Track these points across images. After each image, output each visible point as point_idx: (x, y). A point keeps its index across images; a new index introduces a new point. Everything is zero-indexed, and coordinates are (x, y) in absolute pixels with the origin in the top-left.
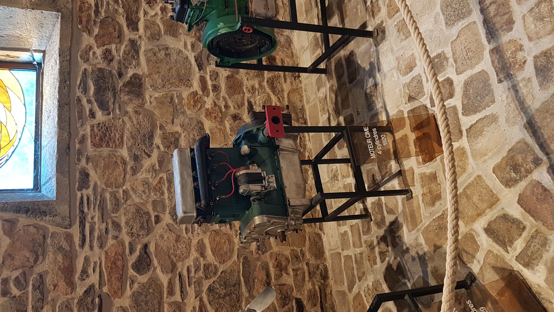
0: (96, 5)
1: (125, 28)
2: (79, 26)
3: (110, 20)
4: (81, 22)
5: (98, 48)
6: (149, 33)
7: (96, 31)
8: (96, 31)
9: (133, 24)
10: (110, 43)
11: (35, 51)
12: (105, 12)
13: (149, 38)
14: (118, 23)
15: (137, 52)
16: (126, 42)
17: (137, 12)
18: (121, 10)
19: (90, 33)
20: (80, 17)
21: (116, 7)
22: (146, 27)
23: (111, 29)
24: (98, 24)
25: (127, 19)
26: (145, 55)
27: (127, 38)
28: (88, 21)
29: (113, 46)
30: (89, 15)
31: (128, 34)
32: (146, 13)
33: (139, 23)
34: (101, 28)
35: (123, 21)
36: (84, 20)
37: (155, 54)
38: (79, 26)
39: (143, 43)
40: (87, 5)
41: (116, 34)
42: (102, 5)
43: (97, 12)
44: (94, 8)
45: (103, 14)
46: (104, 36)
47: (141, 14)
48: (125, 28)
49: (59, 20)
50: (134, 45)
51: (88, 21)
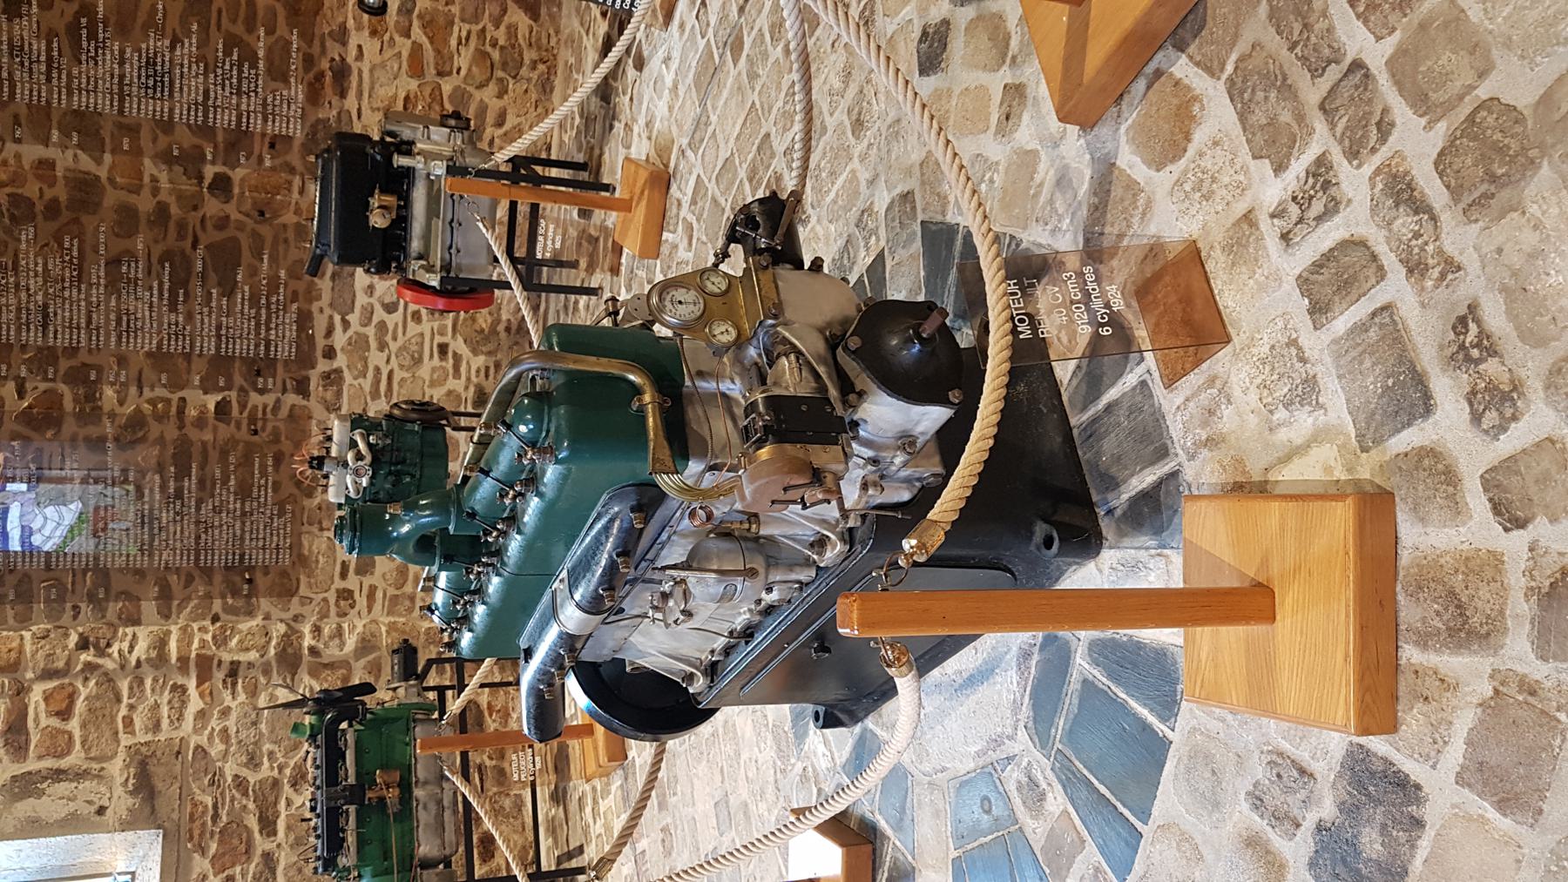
0: (215, 806)
1: (257, 835)
2: (189, 845)
3: (235, 826)
4: (191, 838)
5: (215, 876)
6: (292, 837)
7: (213, 847)
8: (213, 847)
9: (268, 827)
10: (233, 865)
11: (119, 874)
12: (228, 814)
13: (292, 847)
14: (246, 826)
15: (273, 871)
16: (257, 859)
17: (276, 803)
18: (251, 806)
19: (203, 853)
20: (190, 830)
21: (244, 802)
22: (289, 828)
23: (236, 842)
24: (217, 837)
25: (260, 820)
26: (285, 875)
27: (259, 852)
28: (202, 835)
29: (238, 869)
30: (204, 824)
31: (261, 844)
32: (289, 803)
33: (279, 822)
34: (221, 842)
35: (252, 822)
36: (196, 833)
37: (300, 871)
38: (189, 845)
39: (283, 854)
40: (200, 809)
41: (243, 848)
42: (223, 804)
43: (216, 817)
44: (211, 812)
45: (224, 818)
46: (224, 854)
47: (282, 804)
48: (257, 835)
49: (160, 839)
50: (269, 859)
51: (202, 835)
